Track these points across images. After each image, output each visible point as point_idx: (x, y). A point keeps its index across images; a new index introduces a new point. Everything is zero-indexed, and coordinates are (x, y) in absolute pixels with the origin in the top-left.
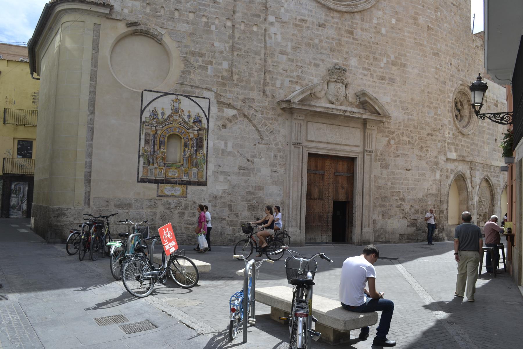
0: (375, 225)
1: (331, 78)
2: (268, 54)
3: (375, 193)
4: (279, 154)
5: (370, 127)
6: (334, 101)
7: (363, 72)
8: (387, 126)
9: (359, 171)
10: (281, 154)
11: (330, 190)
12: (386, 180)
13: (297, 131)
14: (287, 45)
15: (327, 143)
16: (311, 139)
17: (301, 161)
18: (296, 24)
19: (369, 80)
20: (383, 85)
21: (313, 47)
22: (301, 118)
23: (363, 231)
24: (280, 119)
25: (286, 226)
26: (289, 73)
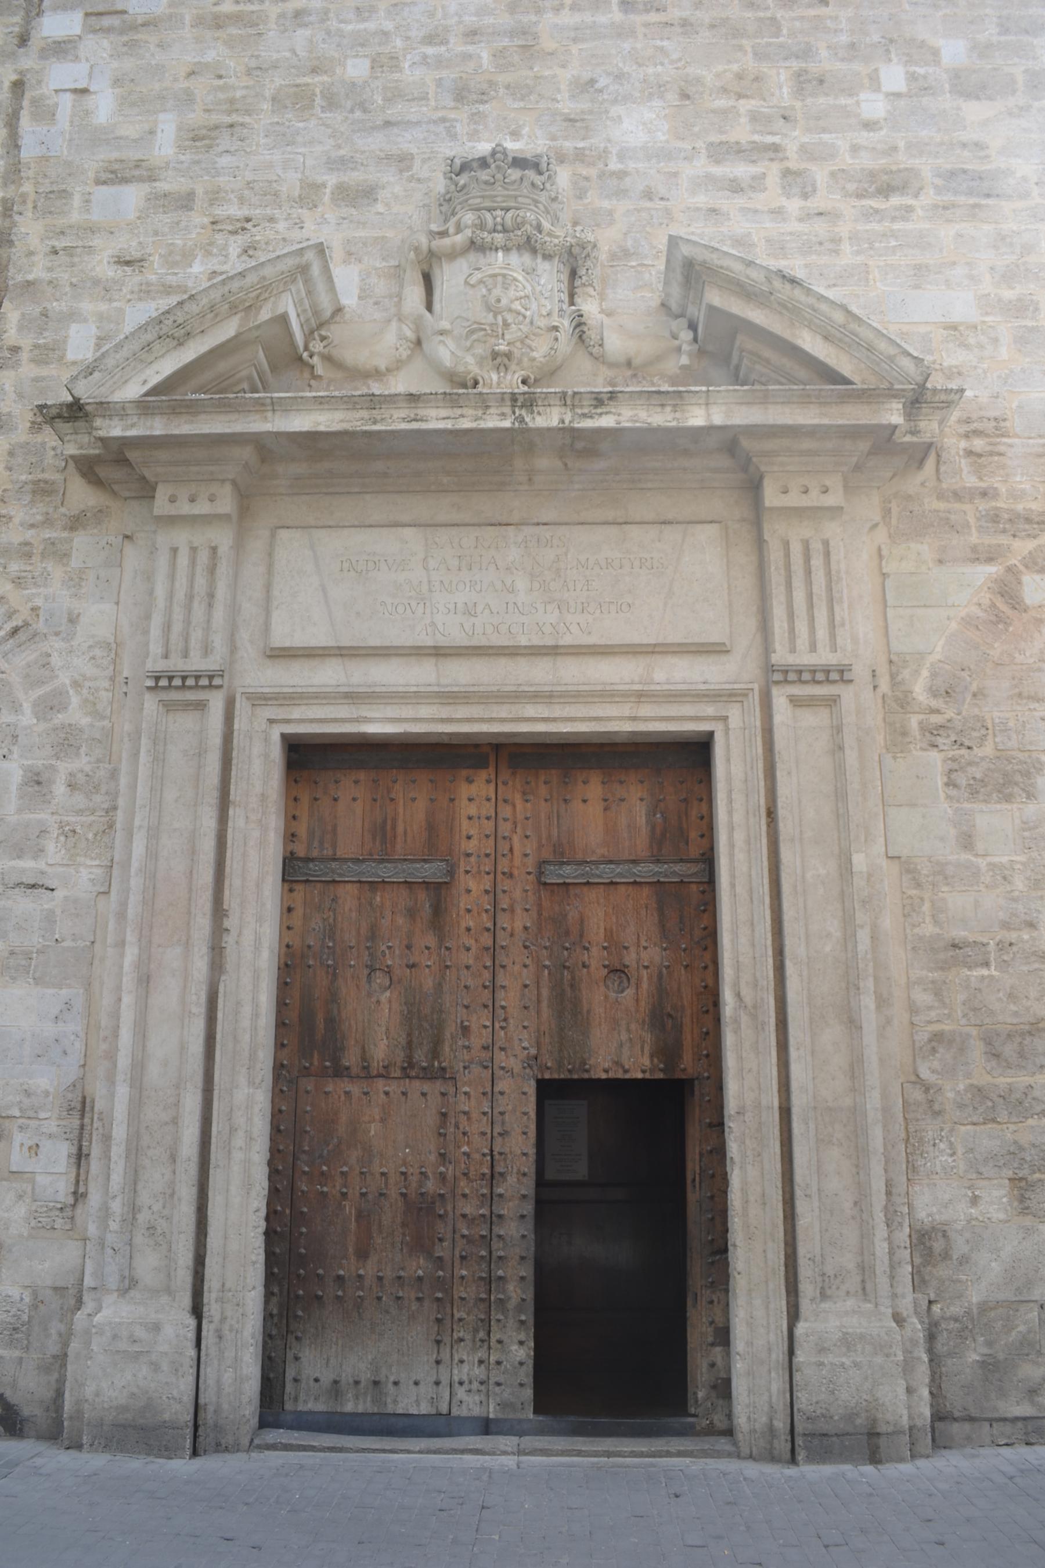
0: (943, 1271)
1: (443, 234)
2: (24, 202)
3: (922, 997)
4: (64, 767)
5: (794, 499)
6: (475, 370)
7: (717, 170)
8: (971, 481)
9: (739, 837)
10: (82, 763)
11: (510, 998)
12: (1019, 884)
13: (180, 595)
14: (152, 132)
15: (439, 653)
16: (300, 639)
17: (212, 797)
18: (216, 17)
19: (778, 213)
20: (897, 226)
21: (331, 102)
22: (202, 508)
23: (801, 1328)
24: (82, 542)
25: (88, 1281)
26: (156, 272)
